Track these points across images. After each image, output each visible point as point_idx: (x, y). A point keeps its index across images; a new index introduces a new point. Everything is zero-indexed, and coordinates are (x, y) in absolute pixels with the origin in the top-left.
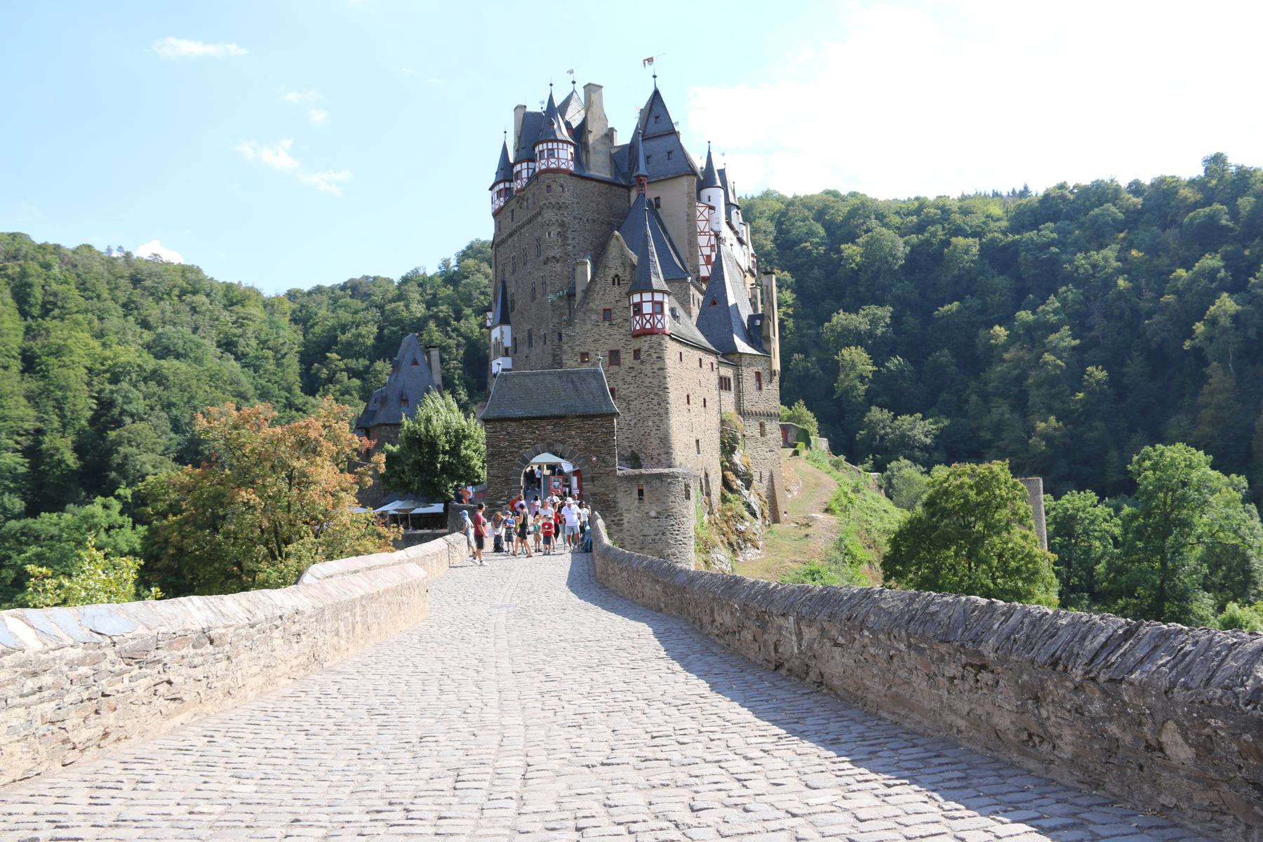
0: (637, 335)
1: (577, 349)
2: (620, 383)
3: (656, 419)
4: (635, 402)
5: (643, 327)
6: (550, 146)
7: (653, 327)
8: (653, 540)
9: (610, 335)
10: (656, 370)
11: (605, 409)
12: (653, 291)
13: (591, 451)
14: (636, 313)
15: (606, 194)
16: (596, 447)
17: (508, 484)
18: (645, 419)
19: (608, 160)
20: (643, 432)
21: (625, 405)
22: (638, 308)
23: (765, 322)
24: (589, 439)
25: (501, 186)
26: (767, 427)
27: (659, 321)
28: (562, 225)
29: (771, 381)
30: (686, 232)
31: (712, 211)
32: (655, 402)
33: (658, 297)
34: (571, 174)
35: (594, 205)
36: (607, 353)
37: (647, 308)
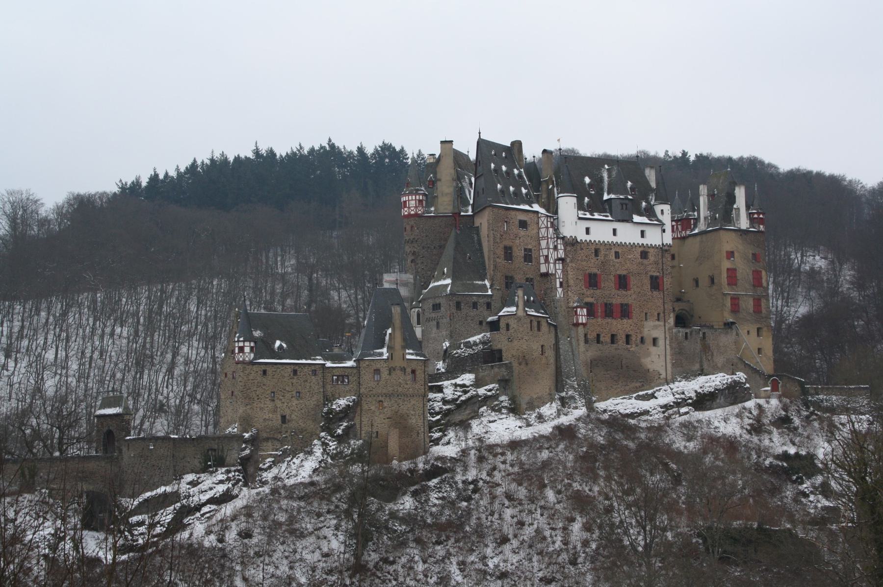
28: (414, 253)
33: (241, 344)
37: (237, 350)
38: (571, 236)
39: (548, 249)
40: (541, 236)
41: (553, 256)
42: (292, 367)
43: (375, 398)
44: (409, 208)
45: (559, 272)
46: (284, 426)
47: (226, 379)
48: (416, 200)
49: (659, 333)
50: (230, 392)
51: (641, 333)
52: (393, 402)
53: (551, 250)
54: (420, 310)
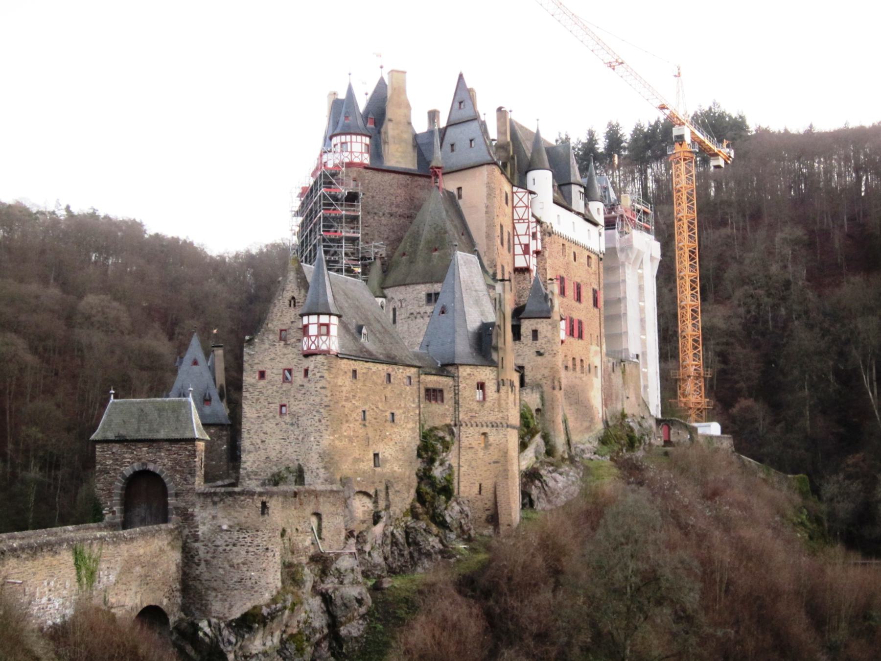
0: (307, 355)
1: (255, 368)
2: (292, 400)
4: (304, 418)
5: (309, 348)
8: (225, 550)
9: (285, 355)
10: (318, 389)
11: (188, 435)
12: (319, 314)
13: (176, 471)
15: (406, 186)
16: (180, 467)
17: (111, 497)
19: (410, 149)
24: (175, 460)
26: (491, 439)
27: (324, 342)
29: (498, 391)
30: (484, 225)
32: (316, 418)
34: (366, 168)
35: (393, 198)
36: (281, 371)
37: (313, 330)
38: (551, 224)
39: (529, 235)
40: (516, 217)
41: (533, 248)
42: (385, 367)
43: (477, 429)
44: (351, 152)
45: (535, 268)
46: (378, 469)
48: (362, 143)
49: (596, 361)
51: (588, 359)
52: (501, 436)
53: (531, 238)
54: (384, 300)
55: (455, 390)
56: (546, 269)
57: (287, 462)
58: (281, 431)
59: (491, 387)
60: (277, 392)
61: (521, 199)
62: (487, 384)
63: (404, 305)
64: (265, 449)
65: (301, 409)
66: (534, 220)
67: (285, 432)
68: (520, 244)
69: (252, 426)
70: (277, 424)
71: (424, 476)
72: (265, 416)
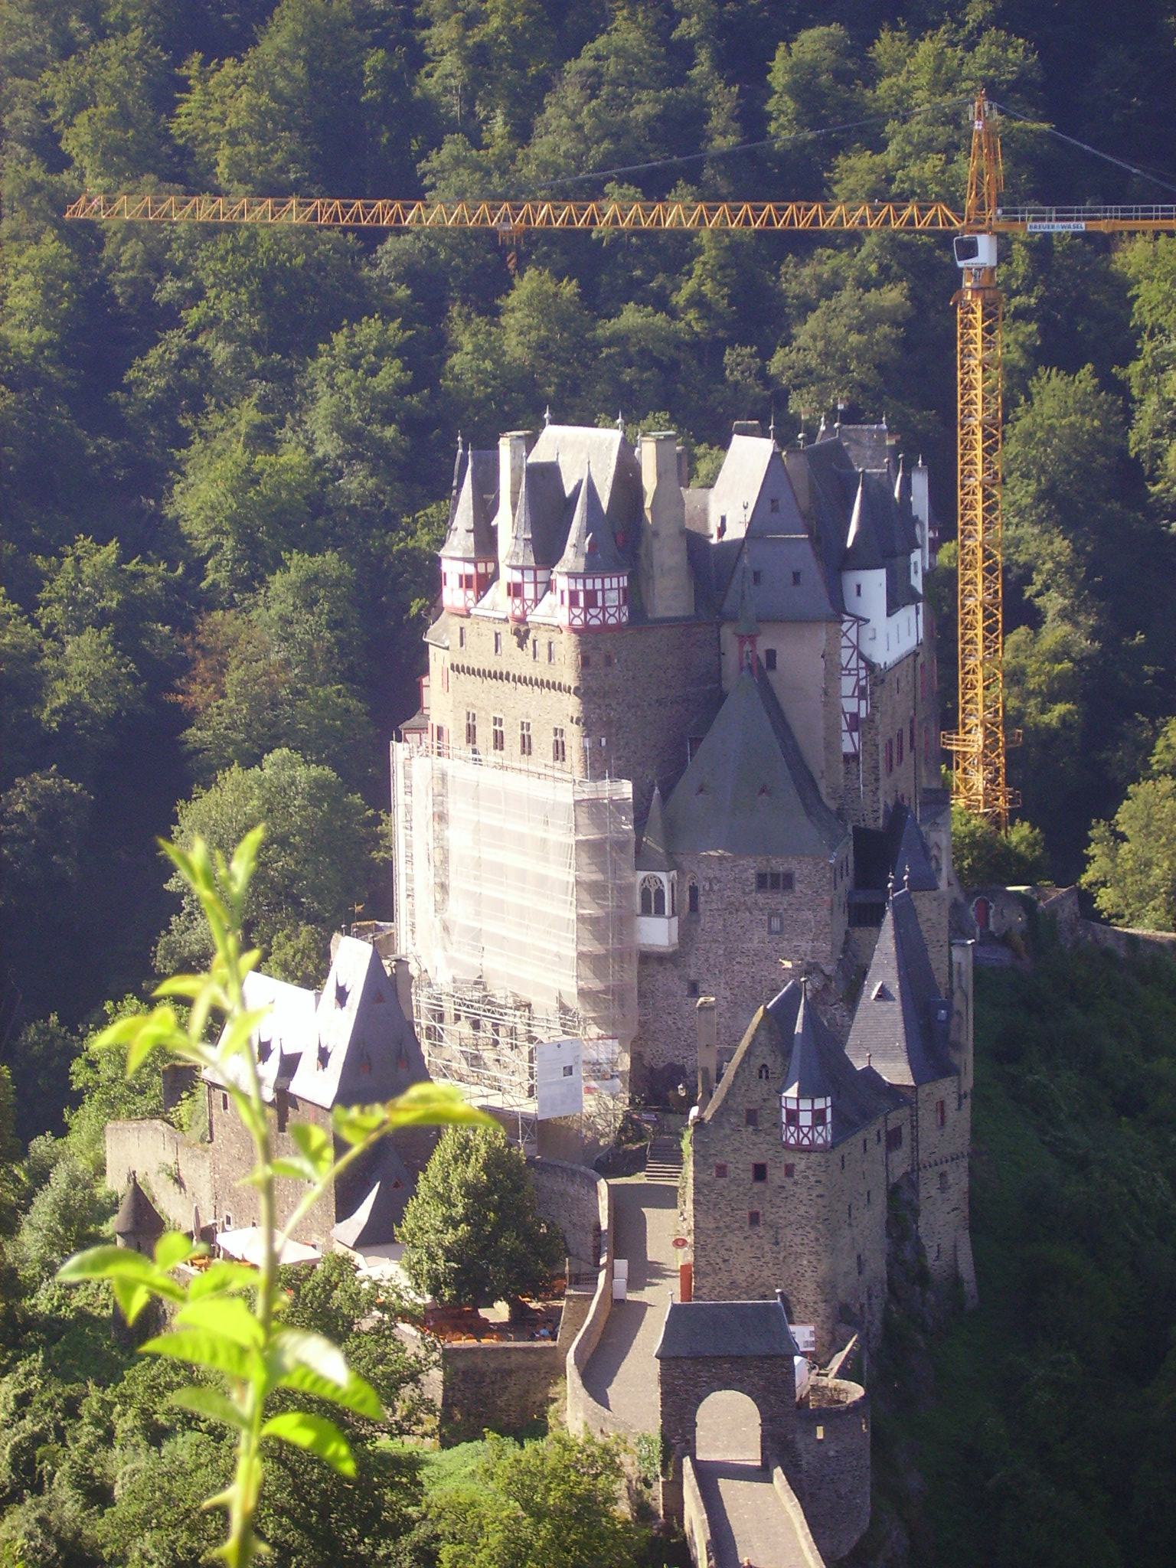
3: (812, 1258)
4: (788, 1231)
5: (798, 1143)
6: (589, 587)
7: (812, 1142)
14: (788, 1124)
18: (799, 1255)
20: (794, 1271)
21: (772, 1233)
22: (793, 1117)
23: (955, 1020)
25: (470, 569)
26: (951, 1179)
29: (959, 1108)
31: (861, 622)
32: (812, 1236)
36: (751, 1167)
37: (805, 1119)
44: (604, 609)
47: (722, 1181)
50: (745, 1214)
55: (912, 1121)
56: (877, 746)
57: (762, 1290)
58: (752, 1246)
59: (951, 1104)
60: (745, 1195)
61: (845, 634)
62: (947, 1102)
63: (716, 888)
64: (730, 1271)
65: (781, 1218)
66: (862, 664)
67: (758, 1248)
68: (844, 713)
69: (709, 1241)
70: (745, 1238)
71: (894, 1261)
72: (727, 1227)
